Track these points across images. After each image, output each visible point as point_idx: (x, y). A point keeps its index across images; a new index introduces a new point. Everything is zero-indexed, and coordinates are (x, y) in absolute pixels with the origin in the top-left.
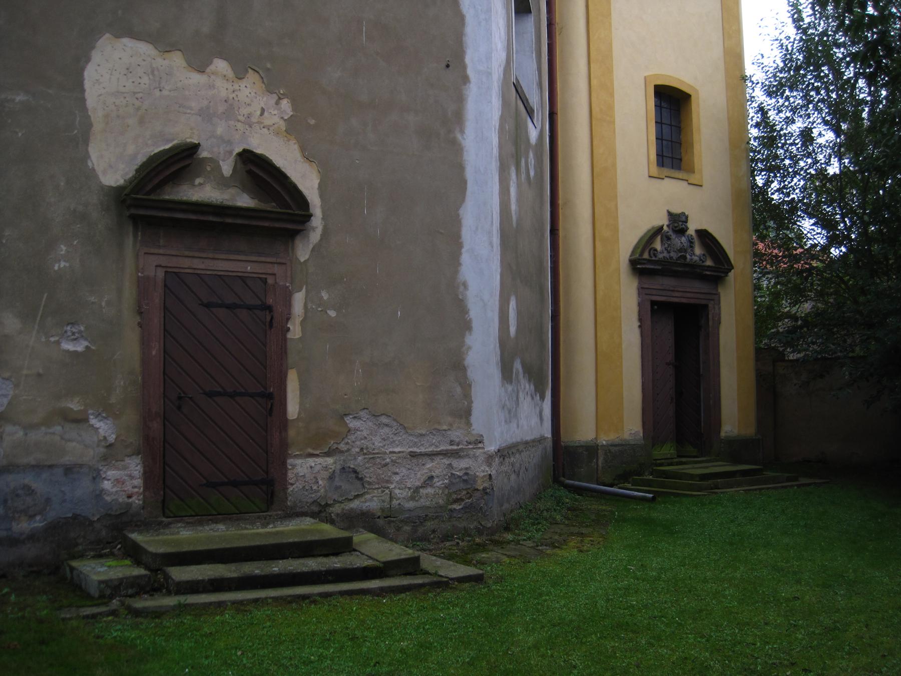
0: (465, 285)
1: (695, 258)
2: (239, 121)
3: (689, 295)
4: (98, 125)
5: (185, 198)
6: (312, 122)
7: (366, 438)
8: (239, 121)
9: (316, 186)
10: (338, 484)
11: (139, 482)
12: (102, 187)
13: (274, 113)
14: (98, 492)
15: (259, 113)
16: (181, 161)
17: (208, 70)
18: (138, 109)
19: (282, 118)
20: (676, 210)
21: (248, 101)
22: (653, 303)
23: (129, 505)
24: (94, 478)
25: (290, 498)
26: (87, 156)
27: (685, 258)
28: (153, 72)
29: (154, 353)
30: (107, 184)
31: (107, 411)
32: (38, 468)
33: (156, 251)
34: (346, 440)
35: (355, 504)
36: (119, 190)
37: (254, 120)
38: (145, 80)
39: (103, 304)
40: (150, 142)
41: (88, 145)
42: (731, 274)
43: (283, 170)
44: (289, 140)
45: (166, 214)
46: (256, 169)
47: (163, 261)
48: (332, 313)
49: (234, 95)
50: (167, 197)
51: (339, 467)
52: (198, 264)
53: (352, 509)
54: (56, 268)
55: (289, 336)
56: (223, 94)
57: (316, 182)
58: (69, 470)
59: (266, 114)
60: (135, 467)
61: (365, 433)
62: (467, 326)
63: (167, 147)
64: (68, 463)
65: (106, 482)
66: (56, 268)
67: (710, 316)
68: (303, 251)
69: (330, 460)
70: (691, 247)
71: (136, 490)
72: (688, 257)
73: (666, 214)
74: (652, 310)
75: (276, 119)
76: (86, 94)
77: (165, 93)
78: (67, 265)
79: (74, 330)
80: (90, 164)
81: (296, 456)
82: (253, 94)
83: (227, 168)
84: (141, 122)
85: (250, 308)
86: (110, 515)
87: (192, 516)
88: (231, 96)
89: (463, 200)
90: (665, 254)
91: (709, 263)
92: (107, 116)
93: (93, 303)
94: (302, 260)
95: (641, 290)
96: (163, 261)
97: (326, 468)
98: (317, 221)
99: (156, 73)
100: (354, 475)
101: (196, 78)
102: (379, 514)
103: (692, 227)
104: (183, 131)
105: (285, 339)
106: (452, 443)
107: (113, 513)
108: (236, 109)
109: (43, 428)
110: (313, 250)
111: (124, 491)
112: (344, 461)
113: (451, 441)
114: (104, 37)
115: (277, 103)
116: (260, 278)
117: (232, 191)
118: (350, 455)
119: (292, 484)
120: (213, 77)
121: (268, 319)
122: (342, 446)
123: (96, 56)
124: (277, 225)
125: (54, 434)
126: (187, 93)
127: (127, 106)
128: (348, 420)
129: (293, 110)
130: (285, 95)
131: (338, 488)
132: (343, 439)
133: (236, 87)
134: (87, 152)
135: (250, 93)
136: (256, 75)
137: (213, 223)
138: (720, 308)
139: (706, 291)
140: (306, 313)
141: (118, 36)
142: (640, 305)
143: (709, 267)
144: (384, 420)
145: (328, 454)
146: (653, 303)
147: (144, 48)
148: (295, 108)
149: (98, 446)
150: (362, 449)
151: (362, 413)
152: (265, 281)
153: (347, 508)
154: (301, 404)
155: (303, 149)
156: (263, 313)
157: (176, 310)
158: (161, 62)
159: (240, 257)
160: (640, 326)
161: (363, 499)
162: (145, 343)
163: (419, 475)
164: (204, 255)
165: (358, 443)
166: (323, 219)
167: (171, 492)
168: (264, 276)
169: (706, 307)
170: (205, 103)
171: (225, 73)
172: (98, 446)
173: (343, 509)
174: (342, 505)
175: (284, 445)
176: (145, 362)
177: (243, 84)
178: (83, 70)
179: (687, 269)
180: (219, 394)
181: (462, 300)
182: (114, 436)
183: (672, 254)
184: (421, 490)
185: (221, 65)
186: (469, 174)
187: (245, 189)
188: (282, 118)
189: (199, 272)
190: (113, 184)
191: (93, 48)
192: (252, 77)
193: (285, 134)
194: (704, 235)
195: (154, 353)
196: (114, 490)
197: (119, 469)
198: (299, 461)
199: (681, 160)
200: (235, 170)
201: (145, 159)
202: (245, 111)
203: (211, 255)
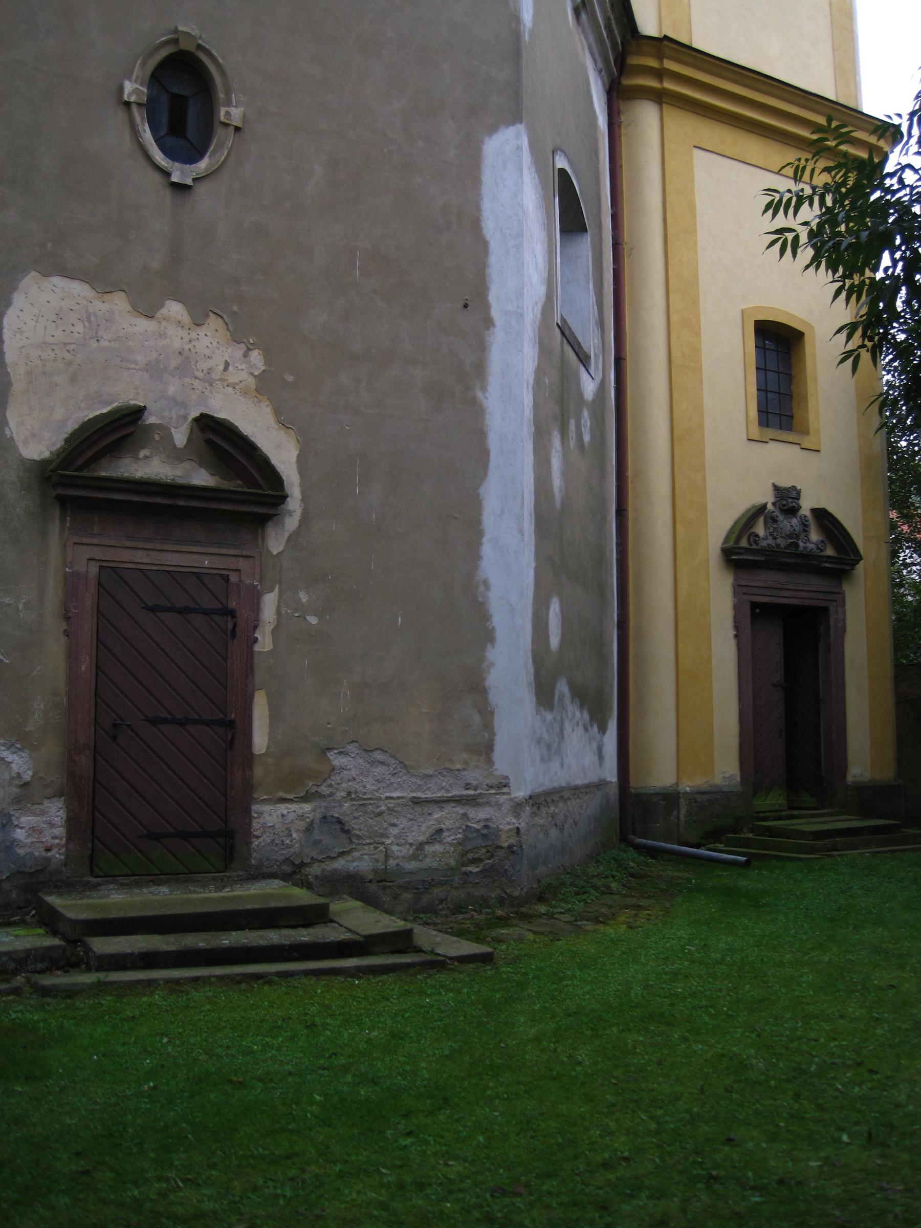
0: (486, 584)
1: (811, 546)
2: (196, 378)
3: (802, 594)
5: (126, 475)
6: (290, 378)
7: (354, 779)
8: (196, 378)
9: (294, 459)
10: (318, 838)
11: (60, 831)
12: (23, 461)
14: (8, 843)
15: (222, 367)
16: (122, 428)
17: (158, 315)
18: (70, 363)
19: (251, 374)
20: (784, 483)
21: (208, 352)
22: (754, 605)
23: (48, 860)
25: (254, 855)
27: (796, 545)
29: (83, 668)
30: (29, 457)
33: (88, 540)
34: (329, 782)
35: (339, 864)
37: (216, 376)
38: (79, 328)
39: (21, 606)
40: (83, 405)
41: (5, 409)
42: (860, 567)
43: (252, 439)
44: (259, 402)
45: (101, 495)
46: (218, 439)
47: (98, 553)
48: (313, 620)
49: (190, 346)
50: (104, 474)
51: (318, 816)
52: (141, 557)
53: (335, 870)
55: (257, 648)
56: (177, 344)
57: (294, 454)
59: (231, 368)
61: (353, 773)
62: (489, 637)
63: (105, 411)
65: (19, 830)
67: (832, 623)
68: (276, 541)
69: (307, 807)
70: (805, 531)
71: (57, 841)
72: (801, 544)
73: (771, 489)
74: (754, 616)
75: (244, 375)
77: (104, 343)
80: (8, 432)
81: (264, 801)
82: (215, 344)
83: (180, 437)
84: (73, 379)
85: (206, 613)
86: (22, 873)
87: (128, 875)
88: (187, 347)
89: (485, 475)
90: (770, 541)
91: (830, 552)
92: (29, 373)
93: (8, 605)
94: (275, 552)
95: (738, 588)
96: (98, 553)
97: (302, 817)
98: (294, 503)
99: (93, 319)
100: (338, 827)
101: (143, 325)
102: (371, 877)
103: (806, 505)
104: (125, 392)
105: (251, 652)
106: (467, 786)
107: (27, 870)
110: (287, 541)
111: (42, 842)
112: (326, 808)
113: (468, 784)
114: (30, 276)
115: (246, 355)
116: (221, 575)
117: (187, 465)
118: (334, 800)
119: (258, 837)
120: (164, 323)
121: (230, 626)
122: (324, 790)
123: (19, 300)
124: (243, 508)
126: (131, 343)
127: (55, 359)
128: (331, 755)
129: (265, 364)
131: (317, 843)
132: (325, 780)
133: (193, 335)
135: (211, 343)
136: (220, 320)
137: (162, 507)
138: (844, 612)
139: (824, 590)
140: (278, 621)
141: (46, 275)
143: (829, 557)
144: (379, 756)
145: (305, 799)
146: (754, 605)
147: (78, 288)
148: (268, 361)
149: (10, 784)
150: (349, 793)
151: (350, 747)
152: (226, 579)
153: (329, 868)
154: (271, 734)
155: (277, 413)
156: (224, 618)
157: (111, 616)
158: (100, 306)
159: (195, 549)
160: (736, 636)
161: (350, 858)
162: (72, 655)
163: (423, 829)
164: (150, 546)
165: (344, 785)
166: (302, 500)
167: (100, 846)
168: (226, 573)
169: (826, 609)
171: (180, 318)
172: (10, 784)
173: (324, 870)
174: (323, 865)
175: (248, 788)
176: (72, 680)
177: (202, 331)
179: (799, 561)
180: (165, 721)
181: (482, 604)
182: (30, 773)
183: (779, 541)
184: (427, 847)
185: (174, 309)
186: (493, 442)
187: (202, 463)
188: (251, 374)
189: (142, 567)
190: (36, 457)
191: (15, 289)
192: (213, 322)
193: (255, 394)
194: (821, 515)
195: (83, 668)
196: (29, 840)
197: (35, 814)
198: (267, 808)
199: (792, 417)
200: (190, 440)
201: (76, 427)
202: (204, 365)
203: (158, 547)
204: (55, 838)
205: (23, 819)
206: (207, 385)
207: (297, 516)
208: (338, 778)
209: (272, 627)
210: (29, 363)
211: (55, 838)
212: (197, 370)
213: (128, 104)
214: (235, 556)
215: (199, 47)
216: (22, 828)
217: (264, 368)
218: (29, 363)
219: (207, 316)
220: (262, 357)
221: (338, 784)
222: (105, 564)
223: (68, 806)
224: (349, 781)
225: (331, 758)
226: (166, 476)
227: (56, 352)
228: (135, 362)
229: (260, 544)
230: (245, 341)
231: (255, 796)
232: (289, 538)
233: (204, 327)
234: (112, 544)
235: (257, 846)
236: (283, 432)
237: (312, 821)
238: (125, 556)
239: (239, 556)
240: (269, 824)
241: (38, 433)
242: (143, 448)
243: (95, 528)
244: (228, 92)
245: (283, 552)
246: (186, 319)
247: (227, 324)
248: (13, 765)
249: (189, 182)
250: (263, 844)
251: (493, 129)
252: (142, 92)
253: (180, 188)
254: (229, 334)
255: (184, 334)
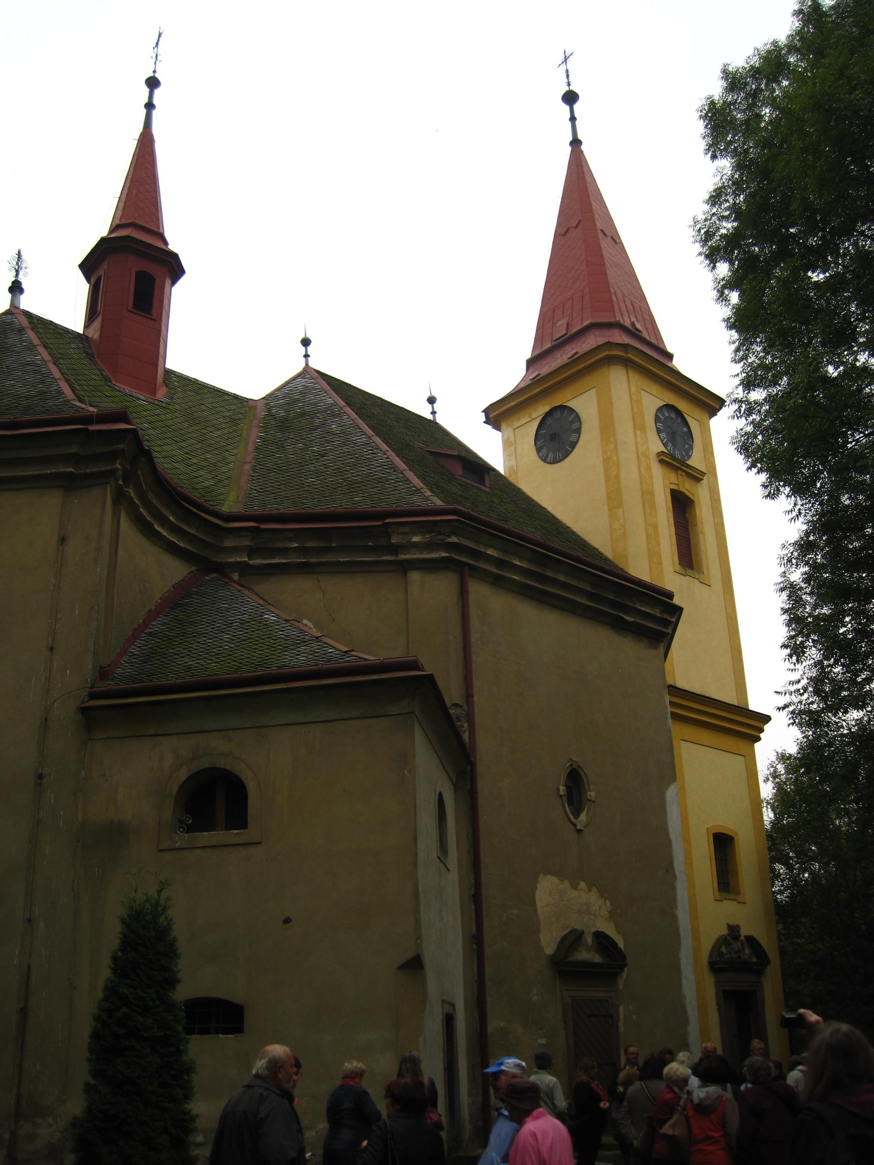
1: (746, 957)
20: (733, 922)
27: (740, 957)
36: (552, 957)
62: (687, 1021)
89: (680, 949)
95: (717, 983)
101: (574, 893)
135: (593, 898)
142: (717, 994)
186: (682, 934)
194: (750, 939)
199: (728, 884)
213: (561, 796)
241: (549, 943)
244: (589, 785)
246: (586, 888)
251: (668, 786)
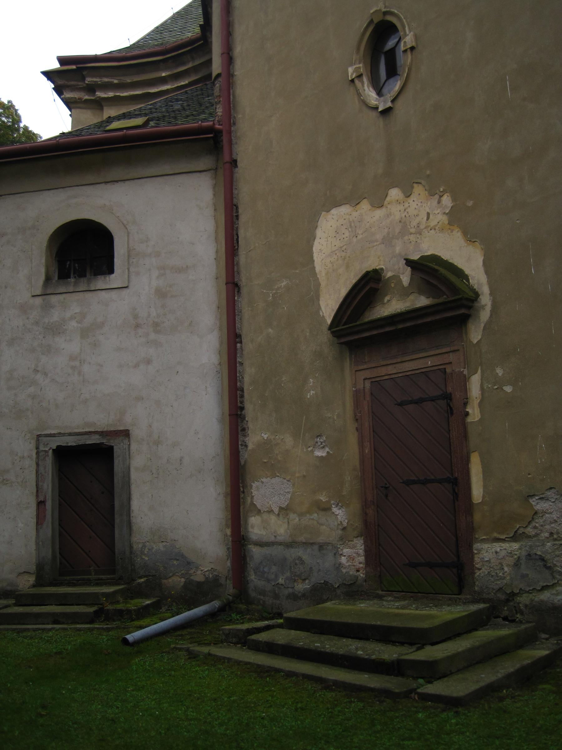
2: (411, 234)
4: (323, 283)
7: (556, 521)
9: (481, 263)
10: (524, 572)
11: (362, 559)
13: (436, 212)
14: (337, 565)
15: (425, 218)
16: (369, 287)
17: (386, 202)
19: (444, 213)
21: (416, 212)
23: (357, 577)
24: (335, 554)
25: (477, 583)
26: (319, 308)
28: (351, 226)
29: (367, 452)
31: (342, 502)
32: (307, 544)
33: (362, 367)
34: (534, 524)
35: (545, 596)
37: (422, 227)
39: (335, 417)
41: (319, 300)
43: (451, 261)
45: (356, 337)
46: (430, 271)
47: (368, 374)
48: (508, 389)
49: (406, 213)
50: (366, 320)
51: (524, 553)
52: (391, 370)
53: (542, 601)
54: (309, 397)
55: (469, 419)
56: (398, 217)
57: (480, 260)
58: (321, 547)
59: (431, 216)
60: (359, 545)
61: (555, 516)
64: (321, 541)
66: (309, 397)
68: (475, 333)
69: (515, 546)
71: (361, 565)
76: (315, 262)
77: (360, 237)
78: (314, 392)
79: (322, 440)
80: (321, 314)
81: (483, 541)
82: (419, 204)
83: (406, 278)
84: (347, 267)
86: (345, 584)
88: (403, 215)
92: (327, 274)
93: (329, 418)
94: (475, 341)
96: (368, 374)
97: (511, 554)
98: (486, 299)
99: (353, 225)
100: (541, 564)
101: (379, 213)
105: (464, 425)
108: (408, 224)
109: (308, 515)
110: (484, 329)
111: (354, 566)
112: (531, 547)
115: (439, 202)
117: (412, 297)
119: (480, 569)
120: (389, 206)
122: (530, 531)
123: (319, 233)
124: (438, 317)
125: (313, 519)
128: (533, 501)
130: (444, 192)
131: (524, 576)
132: (530, 523)
133: (406, 205)
134: (319, 305)
136: (420, 186)
137: (405, 331)
141: (328, 211)
145: (515, 538)
147: (344, 210)
148: (454, 199)
150: (551, 534)
151: (549, 493)
152: (444, 371)
153: (536, 599)
154: (485, 487)
156: (448, 402)
157: (380, 413)
159: (421, 355)
161: (554, 592)
165: (547, 527)
166: (491, 294)
170: (386, 230)
171: (397, 198)
173: (532, 600)
174: (531, 595)
175: (471, 529)
177: (413, 197)
178: (312, 247)
180: (414, 482)
182: (346, 521)
185: (395, 193)
187: (421, 292)
188: (444, 213)
189: (393, 376)
195: (367, 452)
196: (347, 564)
198: (485, 546)
200: (412, 279)
202: (414, 223)
203: (399, 360)
204: (360, 563)
205: (345, 550)
206: (418, 236)
207: (488, 308)
208: (541, 521)
209: (479, 401)
210: (326, 268)
211: (360, 563)
212: (411, 228)
214: (447, 353)
215: (385, 13)
216: (345, 556)
217: (452, 205)
218: (326, 268)
219: (413, 187)
220: (450, 198)
221: (542, 526)
222: (373, 380)
223: (365, 542)
224: (551, 523)
225: (533, 503)
226: (401, 309)
227: (338, 254)
228: (377, 241)
229: (465, 339)
230: (438, 191)
231: (477, 536)
232: (484, 327)
233: (412, 196)
234: (374, 366)
235: (479, 576)
236: (471, 246)
237: (519, 557)
238: (383, 371)
239: (449, 352)
240: (486, 559)
242: (386, 295)
243: (366, 358)
245: (481, 339)
247: (424, 186)
248: (339, 517)
249: (389, 104)
250: (482, 575)
252: (359, 68)
253: (387, 112)
254: (427, 192)
255: (401, 208)
